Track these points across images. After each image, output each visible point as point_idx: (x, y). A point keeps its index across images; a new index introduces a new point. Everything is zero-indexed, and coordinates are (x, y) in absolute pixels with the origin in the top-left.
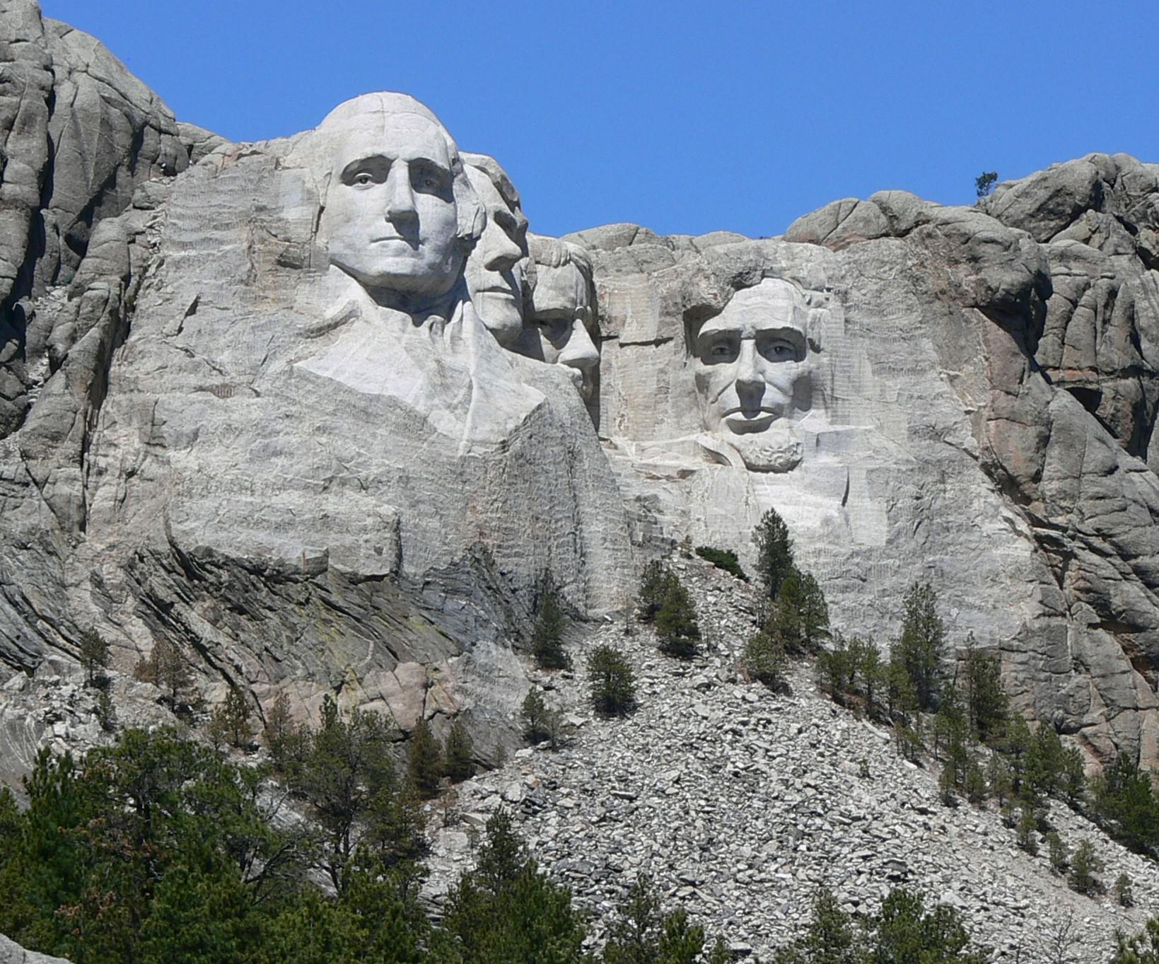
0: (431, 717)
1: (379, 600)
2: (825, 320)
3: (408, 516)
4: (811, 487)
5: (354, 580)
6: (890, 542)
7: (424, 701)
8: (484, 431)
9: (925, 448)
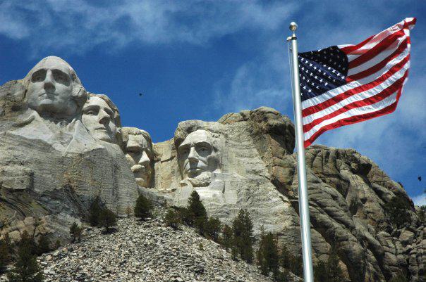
0: (37, 236)
1: (21, 198)
2: (219, 141)
3: (37, 173)
4: (212, 188)
5: (11, 191)
6: (238, 202)
7: (35, 230)
8: (73, 150)
9: (252, 176)
